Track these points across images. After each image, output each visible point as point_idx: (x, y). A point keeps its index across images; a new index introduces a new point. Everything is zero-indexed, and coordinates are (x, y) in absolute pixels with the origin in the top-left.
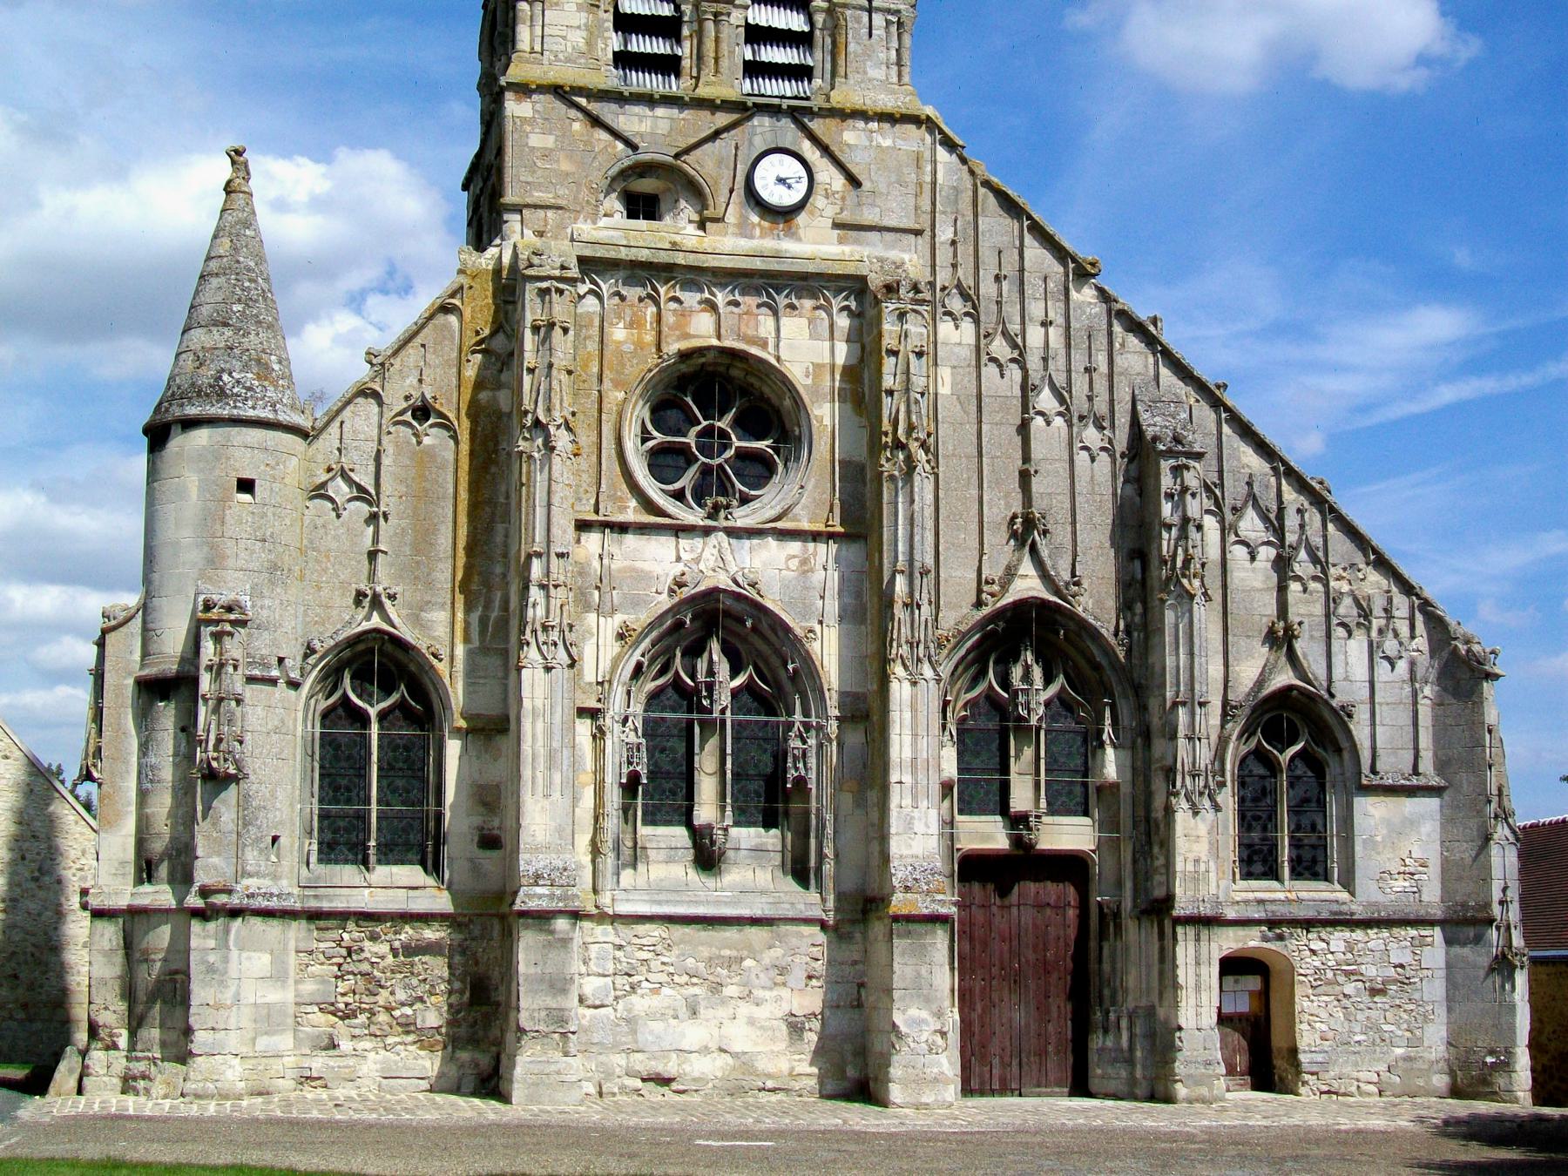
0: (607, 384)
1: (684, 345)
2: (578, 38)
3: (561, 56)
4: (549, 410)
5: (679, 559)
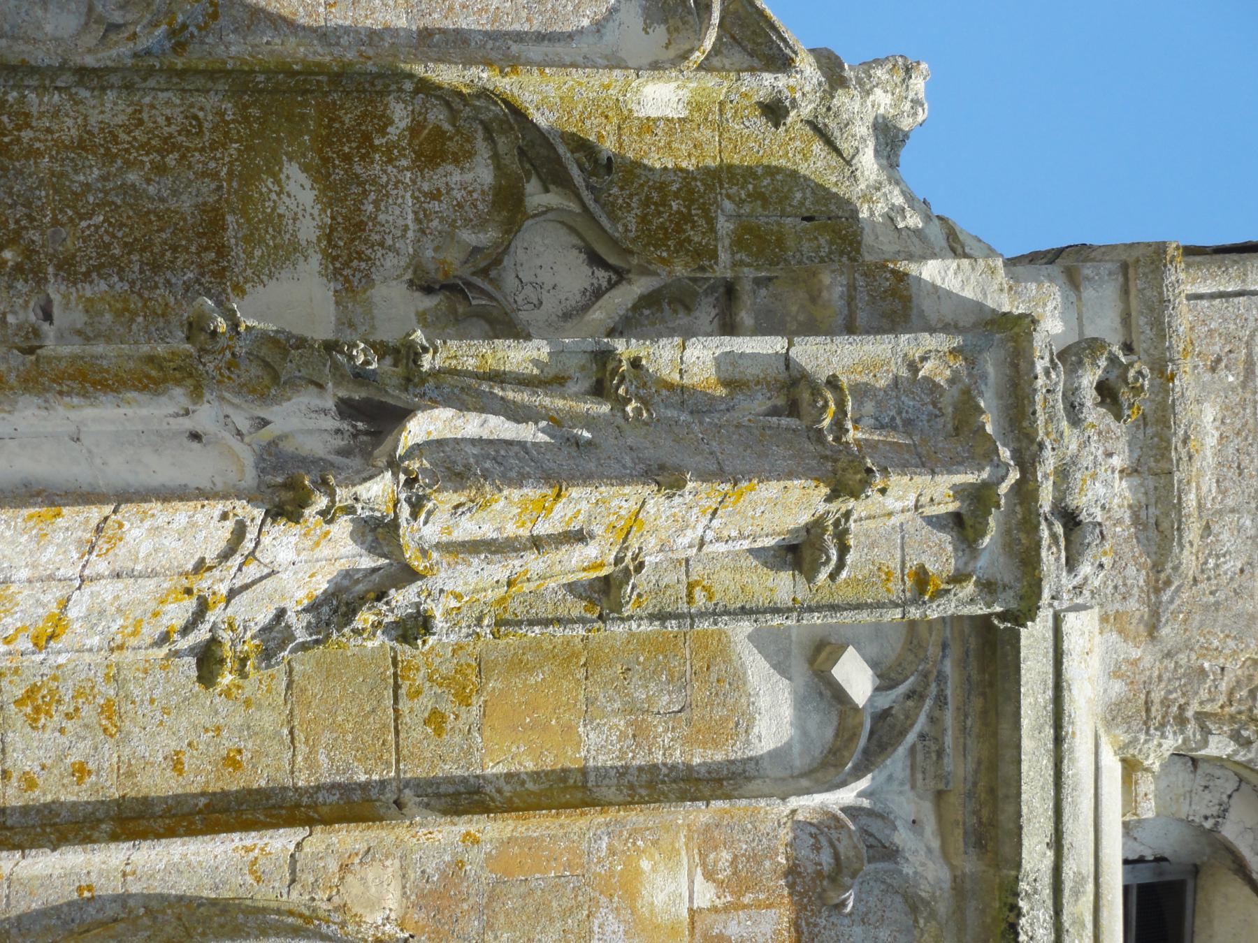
0: (438, 838)
4: (458, 467)
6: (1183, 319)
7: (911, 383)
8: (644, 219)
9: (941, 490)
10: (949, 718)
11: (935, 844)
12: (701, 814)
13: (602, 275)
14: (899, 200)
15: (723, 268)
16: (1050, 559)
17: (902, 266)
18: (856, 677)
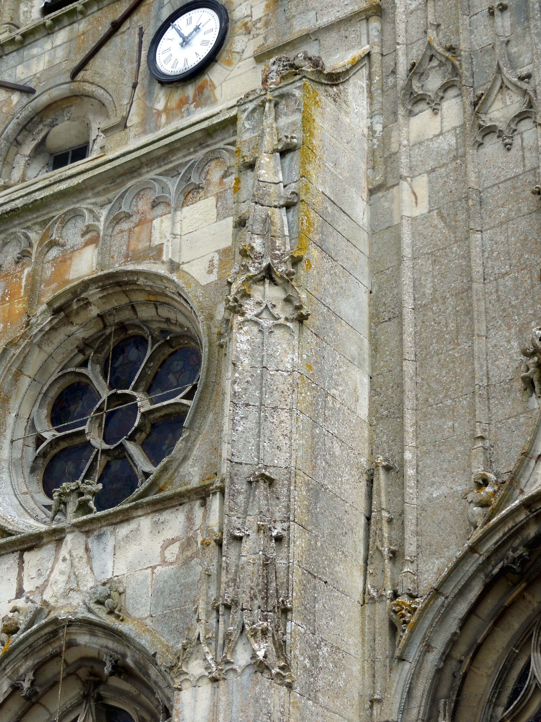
5: (20, 592)
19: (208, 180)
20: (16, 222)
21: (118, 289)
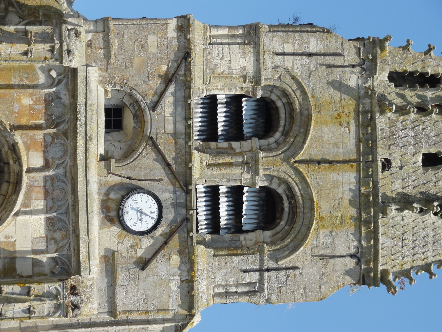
1: (21, 146)
2: (222, 68)
3: (210, 57)
6: (112, 27)
7: (44, 33)
8: (28, 12)
9: (47, 46)
10: (69, 80)
11: (68, 98)
12: (31, 91)
13: (21, 20)
14: (70, 10)
15: (41, 19)
16: (65, 55)
17: (65, 19)
18: (54, 74)
19: (57, 231)
20: (72, 117)
21: (16, 181)
